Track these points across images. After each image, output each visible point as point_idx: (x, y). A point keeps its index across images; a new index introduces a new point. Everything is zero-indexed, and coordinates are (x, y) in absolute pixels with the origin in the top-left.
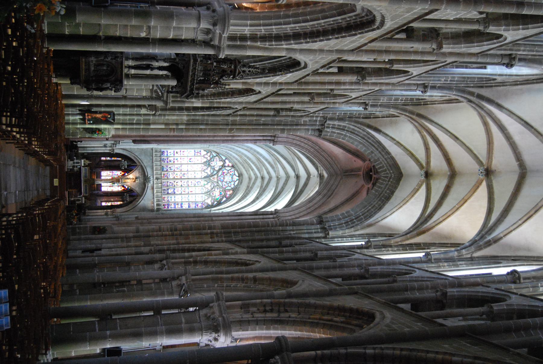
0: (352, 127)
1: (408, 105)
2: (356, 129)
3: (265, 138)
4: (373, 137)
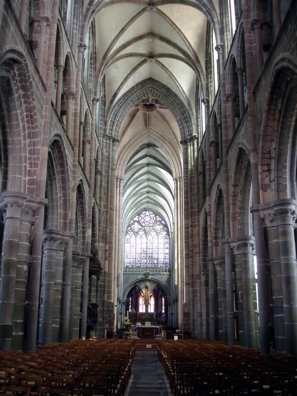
0: (112, 116)
1: (96, 67)
2: (113, 112)
3: (118, 186)
4: (119, 100)
